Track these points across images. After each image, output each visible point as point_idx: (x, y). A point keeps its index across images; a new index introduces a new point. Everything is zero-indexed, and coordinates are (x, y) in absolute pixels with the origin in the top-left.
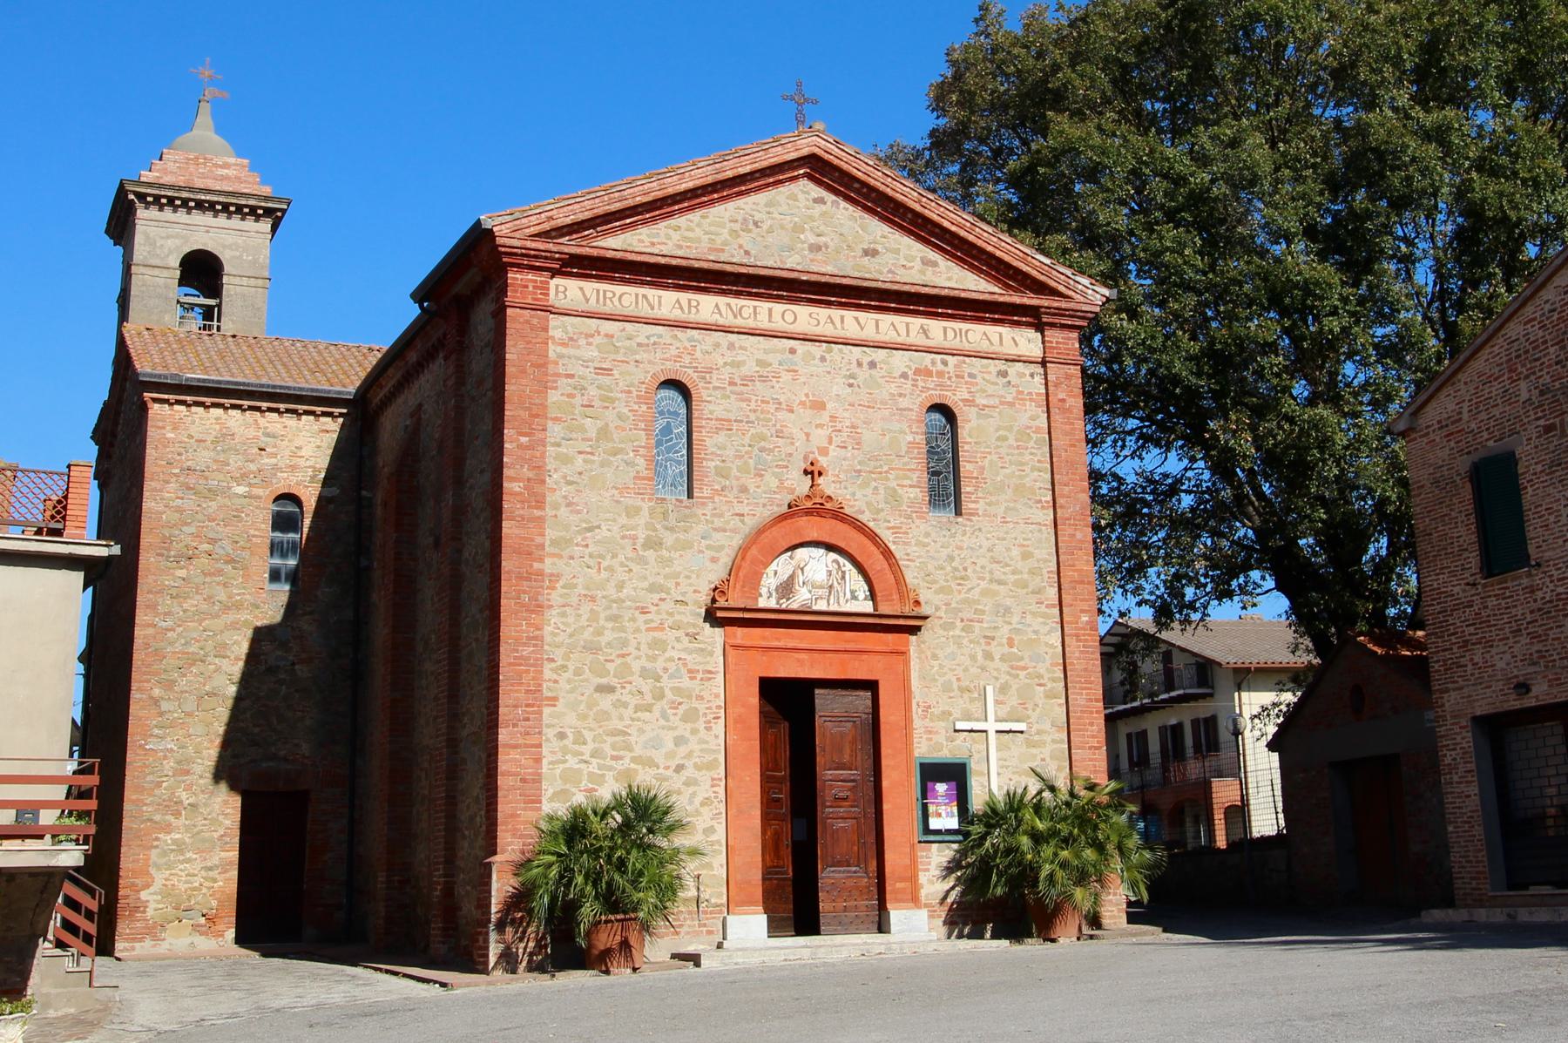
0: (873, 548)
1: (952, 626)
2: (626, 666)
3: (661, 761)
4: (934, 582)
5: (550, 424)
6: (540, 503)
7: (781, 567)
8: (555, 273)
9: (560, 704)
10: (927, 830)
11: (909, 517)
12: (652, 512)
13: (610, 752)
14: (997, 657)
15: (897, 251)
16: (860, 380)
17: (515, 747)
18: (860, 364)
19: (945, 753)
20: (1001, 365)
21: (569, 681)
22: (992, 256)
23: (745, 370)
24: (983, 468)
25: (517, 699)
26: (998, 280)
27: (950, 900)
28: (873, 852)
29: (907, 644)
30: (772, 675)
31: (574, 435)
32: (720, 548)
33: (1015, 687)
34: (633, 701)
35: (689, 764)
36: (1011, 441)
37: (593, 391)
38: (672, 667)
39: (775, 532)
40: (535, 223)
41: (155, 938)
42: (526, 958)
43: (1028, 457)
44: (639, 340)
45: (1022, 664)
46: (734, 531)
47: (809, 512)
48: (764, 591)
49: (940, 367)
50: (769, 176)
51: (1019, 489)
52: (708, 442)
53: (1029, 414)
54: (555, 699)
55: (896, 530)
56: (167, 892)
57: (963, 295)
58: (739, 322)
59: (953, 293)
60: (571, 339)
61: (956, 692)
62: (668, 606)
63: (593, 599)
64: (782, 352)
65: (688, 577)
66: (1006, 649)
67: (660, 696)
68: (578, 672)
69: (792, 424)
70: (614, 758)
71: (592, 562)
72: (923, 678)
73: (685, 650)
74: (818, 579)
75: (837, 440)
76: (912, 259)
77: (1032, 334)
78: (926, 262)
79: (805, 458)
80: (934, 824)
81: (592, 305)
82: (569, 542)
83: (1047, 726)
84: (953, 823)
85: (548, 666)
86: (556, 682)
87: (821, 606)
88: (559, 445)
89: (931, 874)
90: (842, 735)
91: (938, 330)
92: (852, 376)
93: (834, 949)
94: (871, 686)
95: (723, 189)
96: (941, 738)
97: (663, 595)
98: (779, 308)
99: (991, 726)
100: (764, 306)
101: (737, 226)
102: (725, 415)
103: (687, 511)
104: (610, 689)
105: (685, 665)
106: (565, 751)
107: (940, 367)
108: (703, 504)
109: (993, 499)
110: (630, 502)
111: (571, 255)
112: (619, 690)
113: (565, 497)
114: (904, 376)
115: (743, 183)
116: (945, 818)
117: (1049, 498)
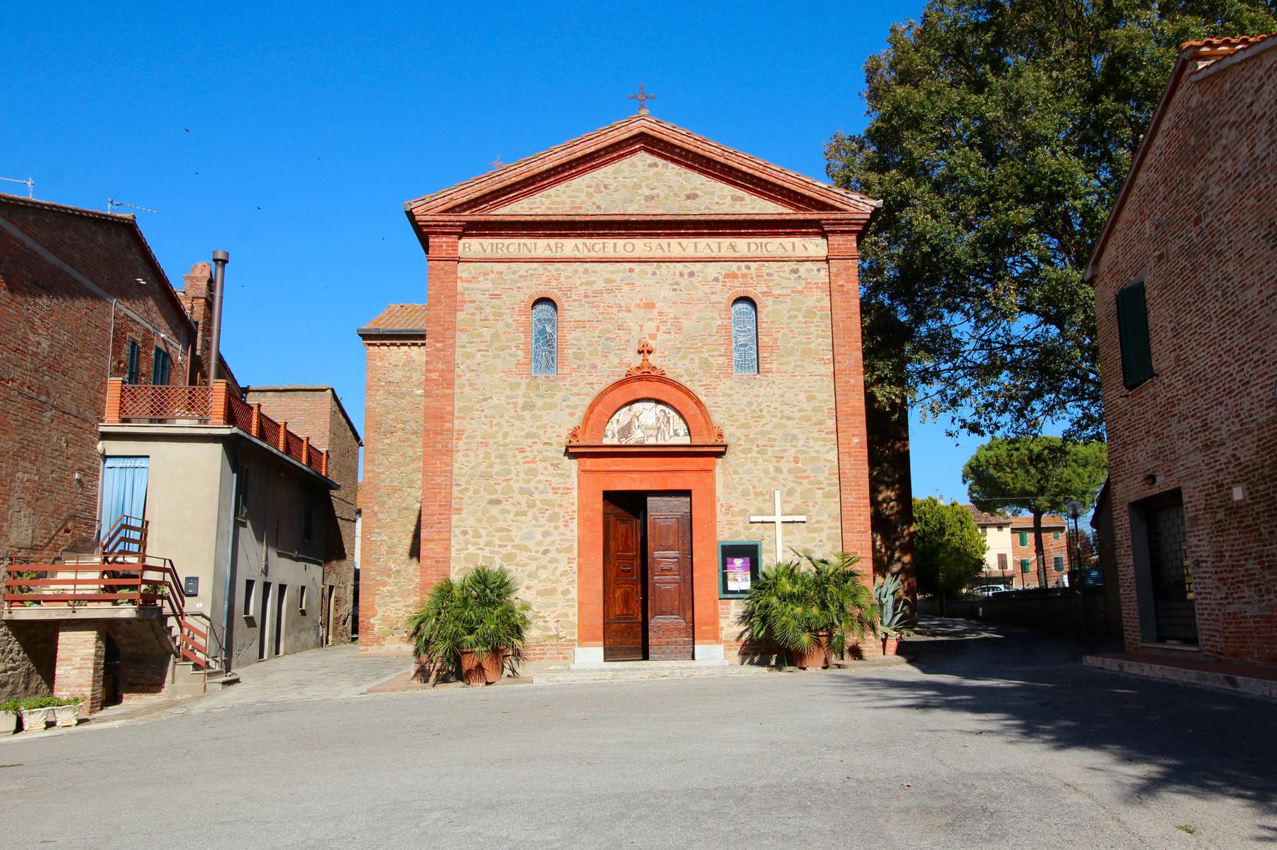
0: (689, 400)
1: (750, 450)
2: (510, 487)
5: (458, 334)
6: (450, 384)
7: (623, 416)
8: (461, 236)
9: (464, 513)
10: (726, 590)
12: (528, 386)
13: (498, 542)
14: (785, 470)
15: (713, 193)
16: (682, 286)
18: (682, 275)
19: (742, 537)
20: (793, 265)
21: (470, 498)
22: (782, 188)
23: (596, 287)
26: (791, 205)
27: (744, 638)
28: (688, 606)
29: (714, 464)
30: (612, 488)
32: (576, 407)
33: (799, 491)
34: (514, 509)
35: (552, 549)
36: (801, 318)
37: (488, 310)
38: (541, 486)
39: (616, 393)
40: (441, 204)
41: (379, 644)
42: (434, 673)
43: (813, 329)
46: (586, 395)
47: (640, 379)
48: (609, 434)
49: (744, 271)
50: (613, 152)
51: (806, 352)
52: (569, 337)
56: (385, 619)
57: (757, 218)
58: (592, 254)
59: (748, 218)
61: (753, 496)
62: (539, 446)
63: (487, 445)
64: (623, 272)
66: (792, 465)
67: (532, 505)
68: (476, 492)
69: (630, 320)
70: (500, 546)
71: (486, 421)
72: (726, 487)
74: (648, 423)
75: (663, 328)
76: (725, 197)
77: (819, 240)
78: (735, 198)
79: (639, 342)
80: (732, 586)
81: (489, 254)
82: (470, 409)
83: (825, 517)
84: (746, 585)
85: (455, 489)
87: (652, 441)
88: (463, 347)
89: (730, 620)
90: (668, 527)
91: (742, 245)
92: (677, 284)
93: (658, 670)
94: (687, 493)
95: (578, 165)
96: (740, 528)
98: (621, 242)
99: (778, 518)
100: (610, 242)
101: (591, 190)
102: (581, 318)
104: (499, 502)
106: (467, 542)
107: (744, 271)
108: (564, 378)
110: (513, 380)
111: (468, 222)
114: (716, 280)
115: (594, 159)
116: (740, 580)
117: (830, 356)
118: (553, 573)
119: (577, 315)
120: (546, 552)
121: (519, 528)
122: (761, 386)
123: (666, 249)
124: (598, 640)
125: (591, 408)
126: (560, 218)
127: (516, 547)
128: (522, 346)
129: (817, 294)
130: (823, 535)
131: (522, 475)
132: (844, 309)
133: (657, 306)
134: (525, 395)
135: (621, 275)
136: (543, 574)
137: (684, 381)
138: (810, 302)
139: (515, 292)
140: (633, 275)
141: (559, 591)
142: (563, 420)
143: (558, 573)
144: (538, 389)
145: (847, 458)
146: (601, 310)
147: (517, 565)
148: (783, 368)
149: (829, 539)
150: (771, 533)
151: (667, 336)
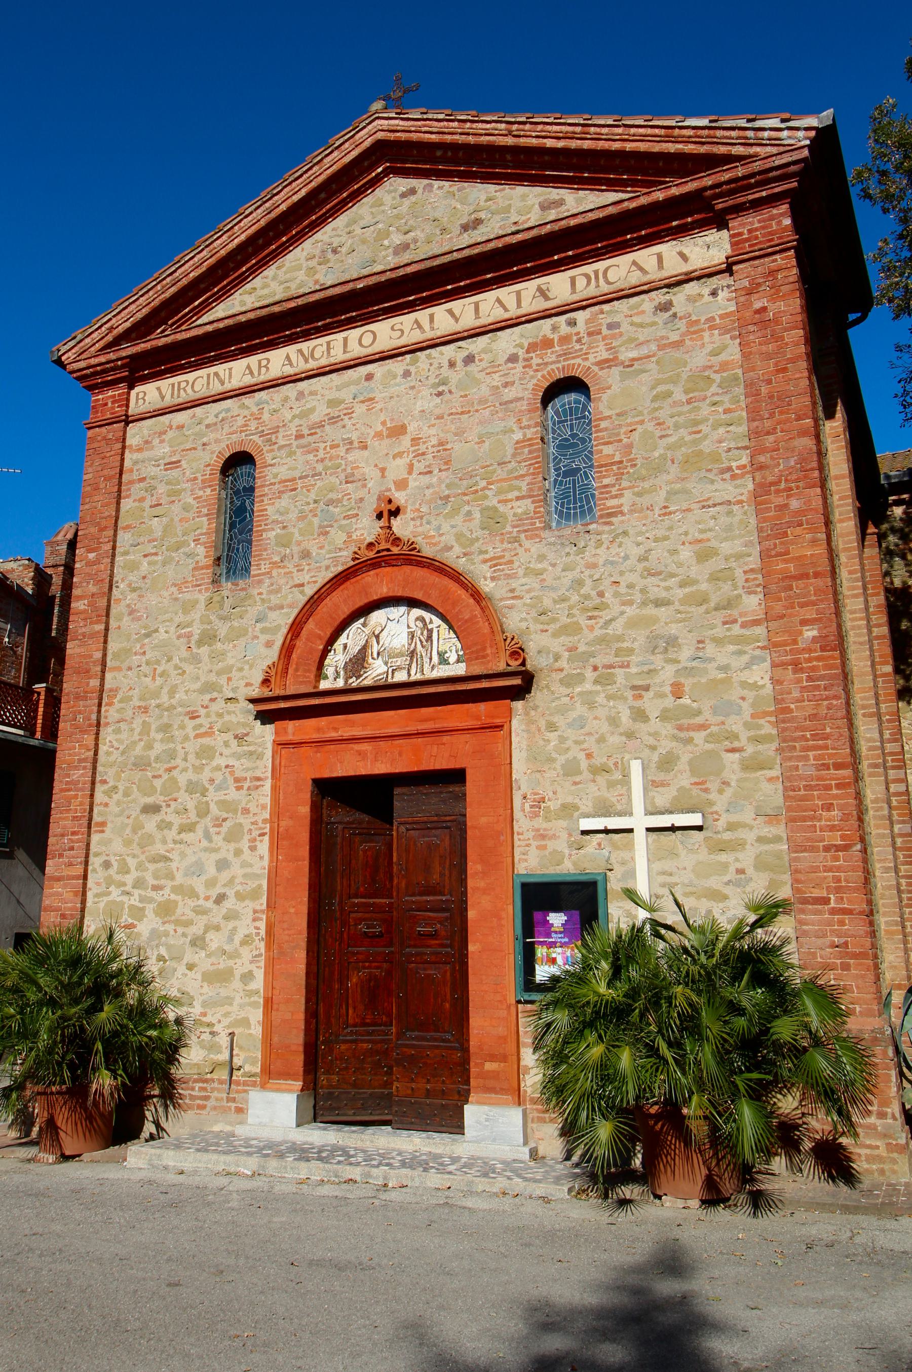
0: (461, 592)
1: (581, 678)
2: (174, 781)
3: (201, 890)
4: (554, 620)
7: (353, 638)
9: (108, 829)
11: (516, 540)
12: (210, 602)
13: (151, 881)
14: (653, 713)
15: (507, 209)
16: (452, 385)
17: (59, 879)
19: (567, 865)
20: (659, 297)
21: (118, 803)
22: (621, 154)
23: (315, 418)
24: (630, 446)
25: (64, 827)
30: (327, 775)
31: (142, 539)
33: (685, 758)
34: (177, 821)
36: (679, 395)
37: (162, 489)
39: (337, 597)
43: (705, 410)
44: (207, 422)
45: (698, 720)
46: (291, 606)
47: (375, 564)
48: (329, 671)
49: (565, 329)
52: (270, 510)
53: (709, 348)
54: (103, 824)
55: (495, 562)
58: (312, 364)
60: (147, 442)
61: (586, 775)
62: (219, 705)
63: (145, 710)
64: (357, 382)
65: (241, 669)
66: (669, 702)
67: (203, 811)
68: (126, 794)
72: (532, 757)
73: (234, 755)
79: (379, 499)
80: (542, 973)
81: (168, 401)
82: (128, 652)
83: (747, 816)
86: (106, 805)
88: (126, 553)
92: (444, 382)
97: (215, 695)
98: (353, 334)
99: (639, 821)
103: (243, 594)
105: (232, 773)
106: (109, 881)
107: (565, 329)
108: (260, 582)
109: (646, 485)
110: (187, 596)
112: (164, 809)
113: (128, 606)
114: (513, 359)
118: (231, 939)
119: (283, 472)
120: (220, 899)
121: (183, 855)
122: (599, 543)
123: (426, 327)
124: (286, 1075)
125: (296, 629)
126: (251, 316)
127: (177, 889)
128: (203, 539)
129: (713, 339)
130: (746, 858)
131: (191, 757)
132: (768, 356)
133: (410, 429)
134: (205, 620)
135: (353, 389)
136: (215, 940)
137: (454, 558)
138: (698, 359)
139: (199, 453)
140: (372, 384)
141: (237, 974)
142: (251, 657)
143: (237, 939)
144: (222, 607)
145: (789, 674)
146: (321, 454)
147: (177, 922)
148: (646, 501)
149: (760, 865)
150: (625, 855)
151: (426, 479)
